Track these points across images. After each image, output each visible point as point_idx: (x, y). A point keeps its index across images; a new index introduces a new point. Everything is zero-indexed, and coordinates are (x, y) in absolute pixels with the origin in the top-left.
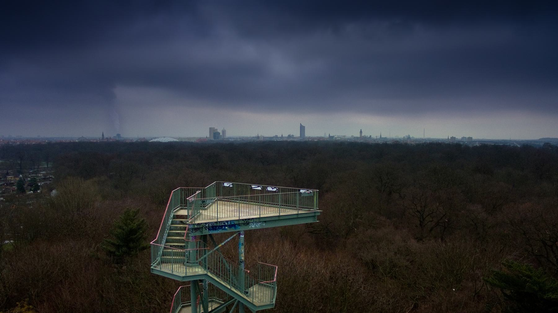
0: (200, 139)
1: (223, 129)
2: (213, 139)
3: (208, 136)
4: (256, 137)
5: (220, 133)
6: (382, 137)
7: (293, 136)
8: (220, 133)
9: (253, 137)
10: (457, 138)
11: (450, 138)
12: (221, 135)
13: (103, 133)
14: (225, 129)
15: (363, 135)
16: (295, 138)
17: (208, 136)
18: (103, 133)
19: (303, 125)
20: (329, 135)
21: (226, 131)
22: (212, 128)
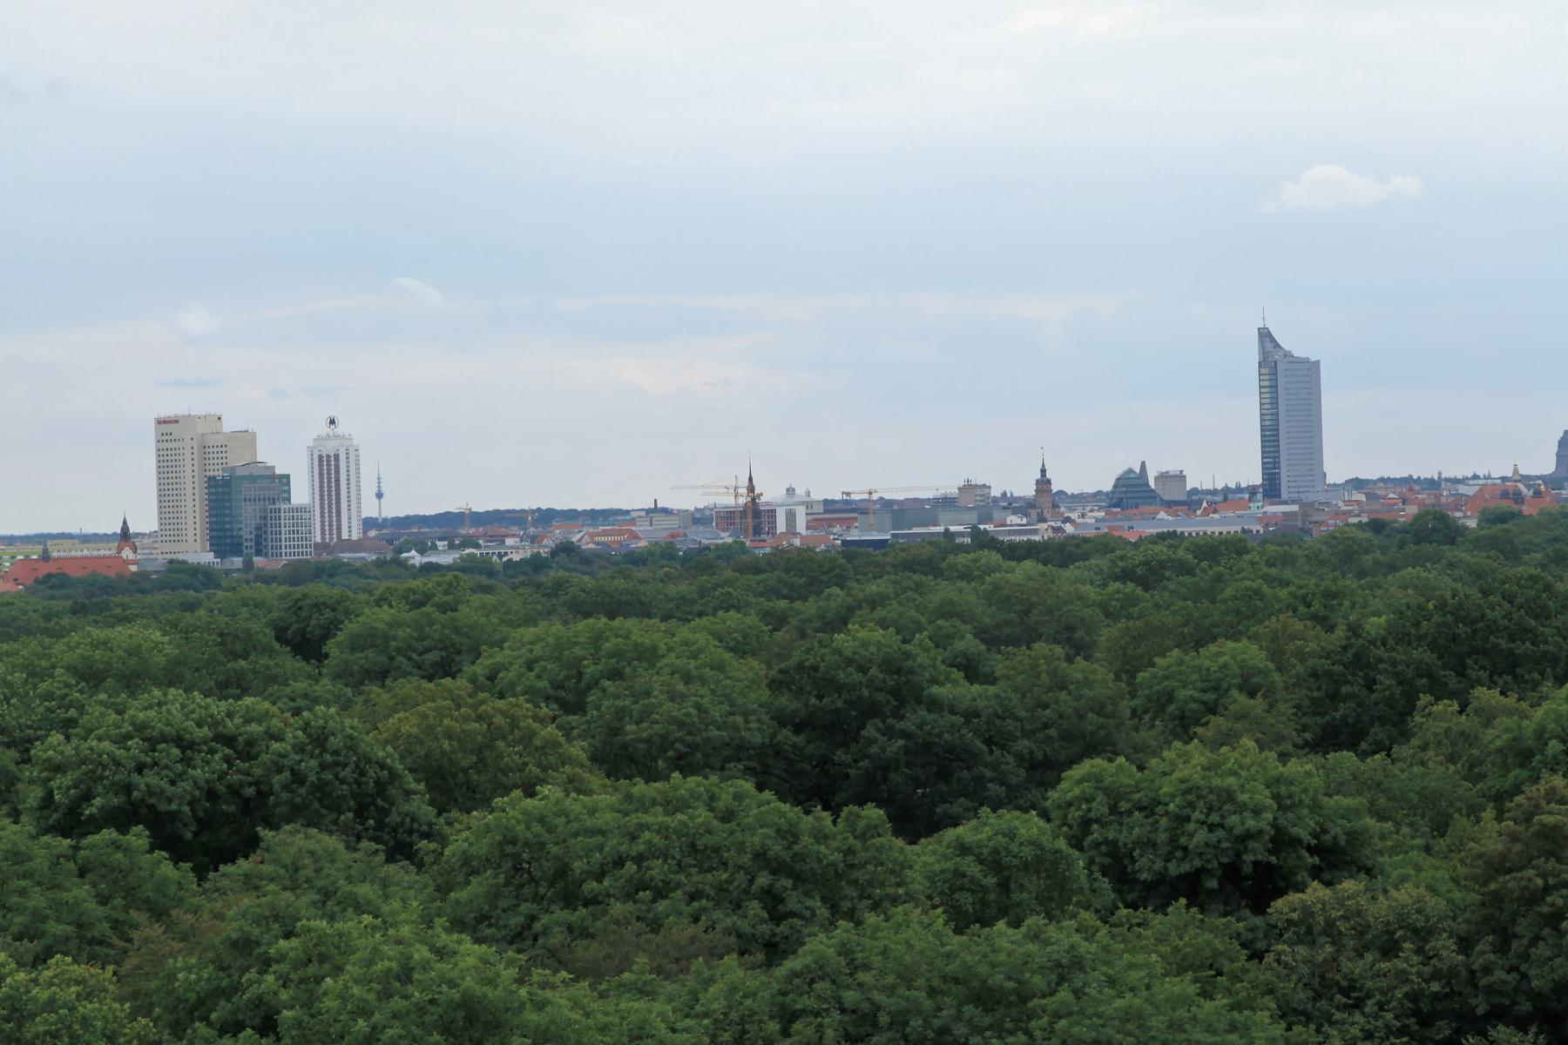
0: (45, 557)
1: (325, 430)
2: (208, 558)
3: (145, 521)
4: (727, 517)
5: (288, 477)
7: (1181, 477)
8: (288, 477)
9: (699, 518)
12: (301, 509)
14: (341, 429)
16: (1192, 502)
17: (145, 521)
19: (1298, 352)
21: (353, 453)
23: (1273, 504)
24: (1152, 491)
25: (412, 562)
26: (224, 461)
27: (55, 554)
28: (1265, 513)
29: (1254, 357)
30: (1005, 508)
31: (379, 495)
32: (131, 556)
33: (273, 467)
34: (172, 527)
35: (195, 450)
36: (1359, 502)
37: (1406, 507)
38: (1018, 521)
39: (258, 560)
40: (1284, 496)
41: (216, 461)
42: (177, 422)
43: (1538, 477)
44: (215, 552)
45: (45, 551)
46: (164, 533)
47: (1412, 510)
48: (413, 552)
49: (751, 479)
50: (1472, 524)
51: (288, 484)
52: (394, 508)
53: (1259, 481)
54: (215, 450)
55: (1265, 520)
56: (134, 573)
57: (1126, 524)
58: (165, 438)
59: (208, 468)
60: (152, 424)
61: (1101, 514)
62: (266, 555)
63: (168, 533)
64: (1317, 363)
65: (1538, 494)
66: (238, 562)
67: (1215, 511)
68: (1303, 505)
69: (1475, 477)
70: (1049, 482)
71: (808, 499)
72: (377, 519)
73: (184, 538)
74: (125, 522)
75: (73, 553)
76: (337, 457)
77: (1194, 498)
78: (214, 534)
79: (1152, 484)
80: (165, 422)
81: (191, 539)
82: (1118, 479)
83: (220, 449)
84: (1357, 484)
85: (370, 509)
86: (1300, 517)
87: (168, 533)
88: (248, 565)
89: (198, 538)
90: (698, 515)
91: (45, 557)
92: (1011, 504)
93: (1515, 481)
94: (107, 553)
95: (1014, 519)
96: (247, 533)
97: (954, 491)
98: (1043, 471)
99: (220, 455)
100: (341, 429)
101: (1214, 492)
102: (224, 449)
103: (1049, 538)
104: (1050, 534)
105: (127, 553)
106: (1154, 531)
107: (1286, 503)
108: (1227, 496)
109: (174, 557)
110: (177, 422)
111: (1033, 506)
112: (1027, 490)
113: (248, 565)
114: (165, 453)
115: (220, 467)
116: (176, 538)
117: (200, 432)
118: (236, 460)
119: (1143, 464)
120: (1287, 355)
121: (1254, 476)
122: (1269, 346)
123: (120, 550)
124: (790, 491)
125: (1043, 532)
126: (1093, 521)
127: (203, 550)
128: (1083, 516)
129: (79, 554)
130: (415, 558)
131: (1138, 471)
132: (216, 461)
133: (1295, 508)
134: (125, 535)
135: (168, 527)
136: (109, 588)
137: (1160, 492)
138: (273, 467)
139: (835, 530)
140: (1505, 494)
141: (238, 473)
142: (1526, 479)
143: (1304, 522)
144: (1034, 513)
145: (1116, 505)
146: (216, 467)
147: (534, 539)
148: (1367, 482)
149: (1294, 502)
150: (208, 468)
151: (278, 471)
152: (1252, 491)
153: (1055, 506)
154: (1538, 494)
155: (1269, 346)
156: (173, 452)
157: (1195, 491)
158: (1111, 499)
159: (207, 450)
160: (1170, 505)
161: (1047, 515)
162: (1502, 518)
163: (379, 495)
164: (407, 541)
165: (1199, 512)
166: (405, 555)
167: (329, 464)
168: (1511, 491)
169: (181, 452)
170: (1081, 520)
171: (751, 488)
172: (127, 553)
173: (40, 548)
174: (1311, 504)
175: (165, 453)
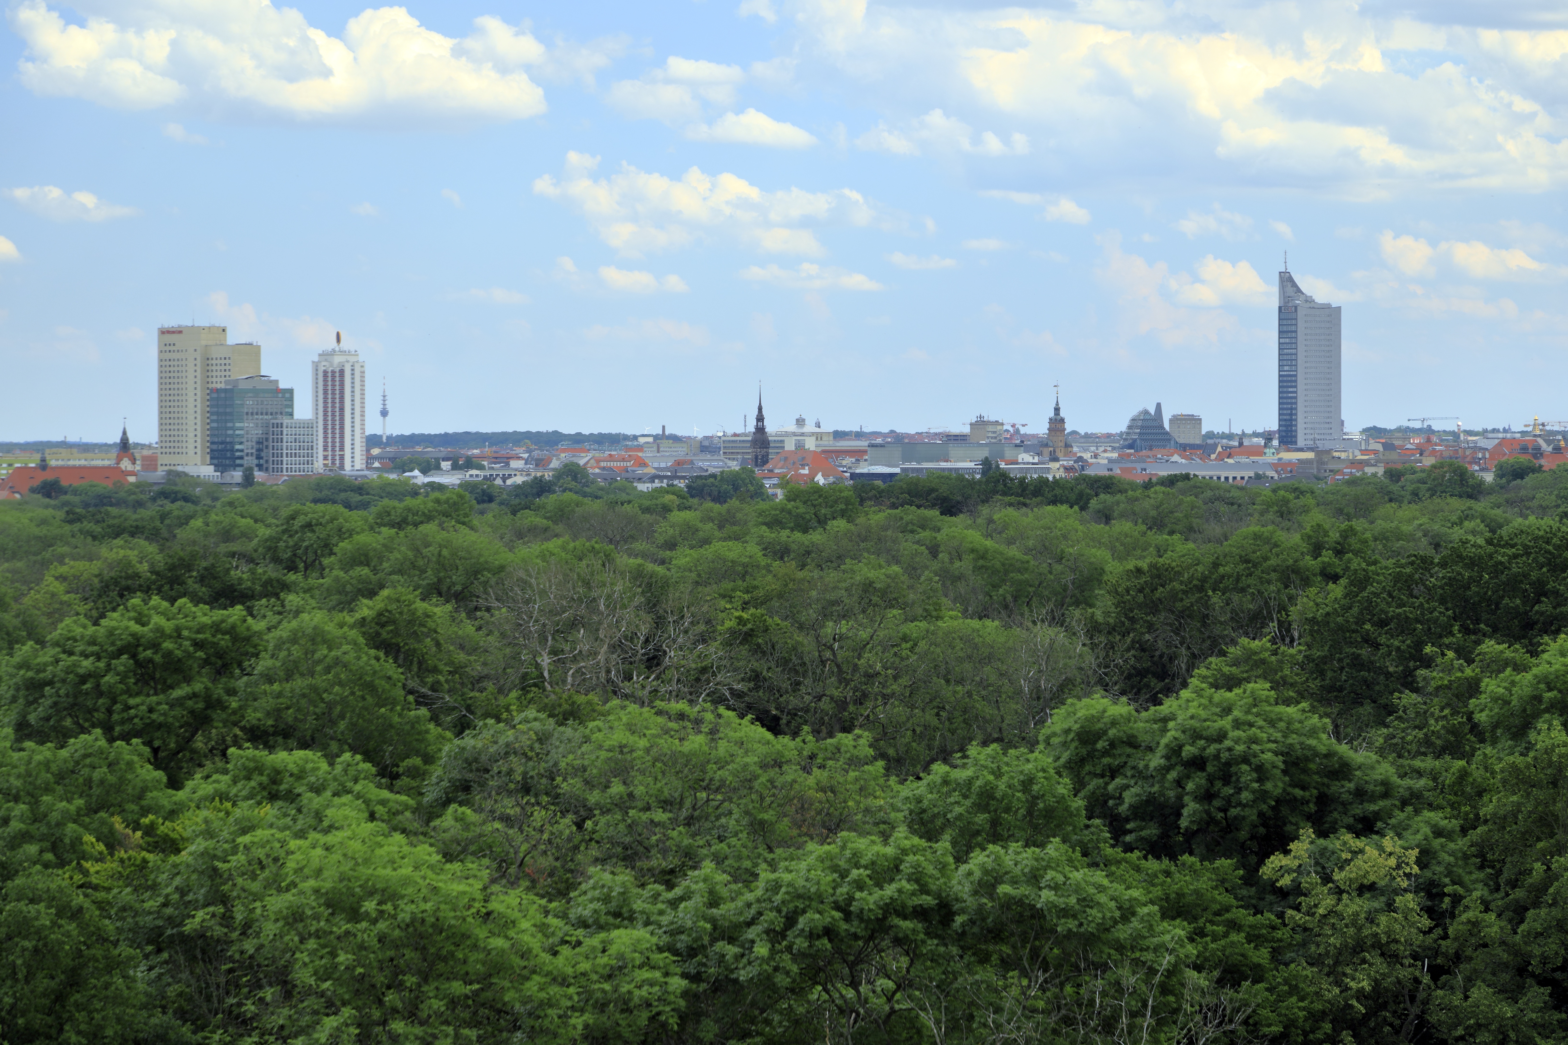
0: (43, 466)
1: (332, 344)
2: (207, 471)
5: (291, 391)
7: (1194, 421)
8: (291, 391)
9: (707, 446)
12: (308, 426)
14: (345, 345)
22: (195, 330)
23: (1289, 450)
24: (1167, 433)
25: (415, 481)
26: (227, 373)
27: (53, 463)
28: (1280, 459)
29: (1274, 303)
30: (1017, 446)
31: (384, 413)
32: (130, 467)
33: (277, 381)
34: (172, 439)
35: (198, 362)
36: (1375, 452)
37: (1423, 458)
38: (1031, 460)
40: (1301, 443)
41: (219, 374)
42: (180, 332)
43: (1558, 433)
44: (215, 465)
45: (43, 460)
46: (164, 445)
47: (1428, 461)
48: (416, 472)
49: (760, 409)
50: (1489, 477)
51: (291, 399)
53: (1274, 425)
54: (219, 362)
55: (1278, 466)
56: (131, 484)
57: (1139, 466)
58: (168, 348)
59: (210, 380)
60: (155, 335)
61: (1115, 455)
62: (267, 469)
63: (168, 444)
65: (1557, 450)
66: (237, 475)
67: (1229, 457)
68: (1319, 453)
69: (1494, 431)
70: (1062, 421)
71: (817, 430)
72: (381, 436)
73: (184, 450)
74: (124, 433)
75: (71, 463)
76: (342, 372)
77: (1210, 441)
78: (215, 447)
79: (1167, 426)
80: (168, 332)
81: (191, 452)
82: (1133, 420)
83: (223, 362)
84: (1373, 432)
85: (374, 426)
86: (1315, 465)
87: (168, 444)
88: (248, 480)
89: (199, 450)
90: (706, 443)
91: (43, 466)
92: (1023, 443)
93: (1535, 436)
94: (106, 463)
95: (1025, 457)
96: (246, 447)
97: (966, 430)
98: (1057, 410)
99: (223, 368)
100: (345, 345)
101: (1230, 437)
102: (227, 361)
103: (1061, 478)
104: (1060, 474)
105: (126, 464)
106: (1164, 473)
107: (1301, 450)
109: (172, 468)
110: (180, 332)
111: (1046, 445)
113: (248, 480)
114: (168, 363)
115: (223, 379)
116: (177, 450)
117: (204, 343)
118: (239, 374)
119: (1159, 406)
120: (1309, 300)
121: (1272, 423)
122: (1290, 291)
123: (119, 460)
124: (800, 422)
125: (1055, 471)
126: (1106, 461)
127: (203, 463)
128: (1096, 456)
129: (77, 463)
130: (419, 478)
131: (1153, 412)
132: (219, 374)
133: (1310, 455)
134: (124, 445)
135: (168, 439)
136: (104, 500)
137: (1175, 435)
138: (277, 381)
139: (844, 463)
140: (1524, 449)
141: (242, 386)
142: (1549, 436)
143: (1319, 470)
144: (1046, 451)
145: (1130, 447)
146: (219, 379)
148: (1385, 430)
149: (1310, 449)
150: (210, 380)
151: (282, 385)
152: (1268, 437)
153: (1068, 446)
154: (1557, 450)
155: (1290, 291)
156: (176, 363)
157: (1210, 435)
158: (1125, 440)
159: (210, 362)
160: (1184, 448)
161: (1060, 455)
163: (384, 413)
164: (411, 461)
165: (1213, 456)
166: (407, 474)
167: (333, 380)
168: (1530, 447)
169: (184, 363)
170: (1094, 460)
171: (760, 418)
172: (126, 464)
173: (37, 457)
174: (1329, 452)
175: (168, 363)
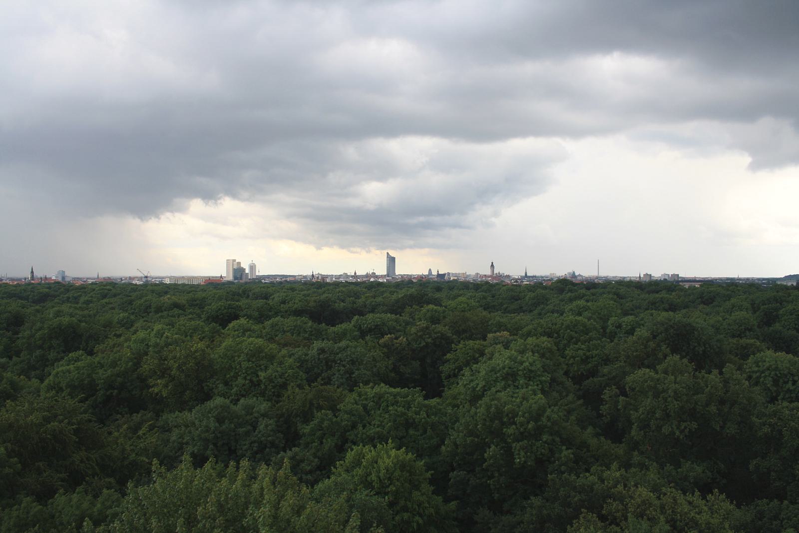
0: (209, 279)
1: (251, 262)
5: (245, 269)
6: (528, 275)
8: (245, 269)
10: (653, 277)
11: (642, 276)
13: (32, 269)
15: (496, 271)
16: (377, 277)
17: (224, 275)
18: (32, 269)
20: (438, 271)
21: (255, 266)
39: (240, 281)
52: (261, 274)
64: (395, 258)
91: (209, 279)
105: (221, 279)
108: (382, 276)
112: (353, 274)
121: (385, 273)
125: (354, 281)
142: (424, 275)
147: (281, 279)
152: (385, 275)
162: (421, 281)
